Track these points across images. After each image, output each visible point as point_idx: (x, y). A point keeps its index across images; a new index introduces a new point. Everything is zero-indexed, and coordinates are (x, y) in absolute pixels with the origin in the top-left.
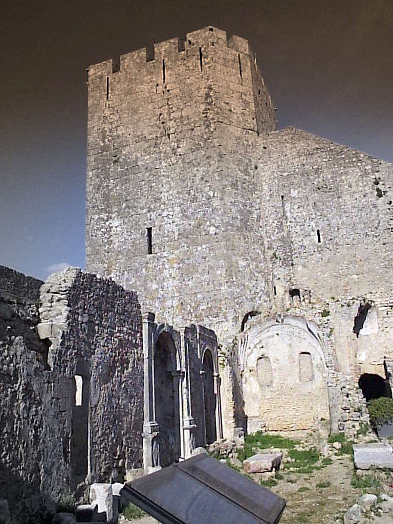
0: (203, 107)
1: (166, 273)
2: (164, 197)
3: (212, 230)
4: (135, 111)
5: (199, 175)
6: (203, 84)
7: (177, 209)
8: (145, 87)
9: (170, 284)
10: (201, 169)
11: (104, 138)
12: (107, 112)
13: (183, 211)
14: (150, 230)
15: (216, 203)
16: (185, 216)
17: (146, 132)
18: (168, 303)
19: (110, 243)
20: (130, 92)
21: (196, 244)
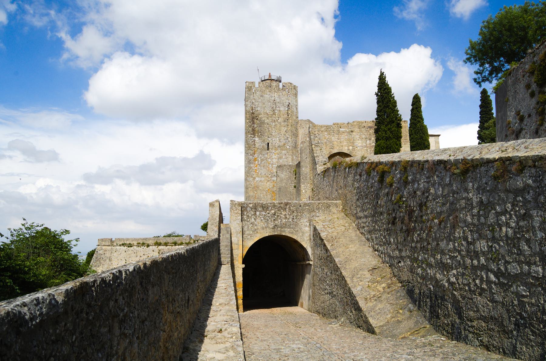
0: (287, 109)
1: (273, 157)
2: (273, 134)
3: (288, 147)
4: (264, 104)
5: (285, 130)
6: (287, 101)
7: (278, 139)
8: (267, 96)
9: (275, 161)
10: (286, 128)
11: (252, 110)
12: (254, 101)
13: (280, 140)
14: (268, 143)
15: (289, 139)
16: (280, 141)
17: (268, 112)
18: (274, 166)
19: (255, 145)
20: (262, 96)
21: (282, 150)
